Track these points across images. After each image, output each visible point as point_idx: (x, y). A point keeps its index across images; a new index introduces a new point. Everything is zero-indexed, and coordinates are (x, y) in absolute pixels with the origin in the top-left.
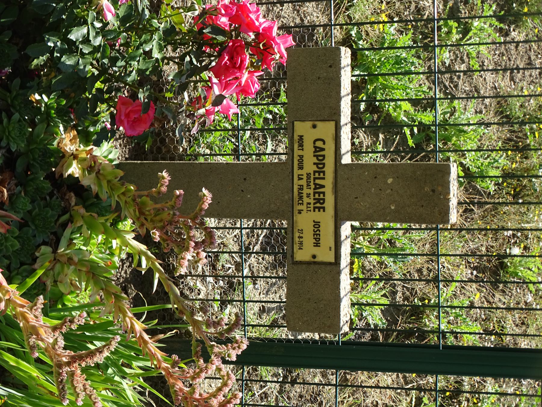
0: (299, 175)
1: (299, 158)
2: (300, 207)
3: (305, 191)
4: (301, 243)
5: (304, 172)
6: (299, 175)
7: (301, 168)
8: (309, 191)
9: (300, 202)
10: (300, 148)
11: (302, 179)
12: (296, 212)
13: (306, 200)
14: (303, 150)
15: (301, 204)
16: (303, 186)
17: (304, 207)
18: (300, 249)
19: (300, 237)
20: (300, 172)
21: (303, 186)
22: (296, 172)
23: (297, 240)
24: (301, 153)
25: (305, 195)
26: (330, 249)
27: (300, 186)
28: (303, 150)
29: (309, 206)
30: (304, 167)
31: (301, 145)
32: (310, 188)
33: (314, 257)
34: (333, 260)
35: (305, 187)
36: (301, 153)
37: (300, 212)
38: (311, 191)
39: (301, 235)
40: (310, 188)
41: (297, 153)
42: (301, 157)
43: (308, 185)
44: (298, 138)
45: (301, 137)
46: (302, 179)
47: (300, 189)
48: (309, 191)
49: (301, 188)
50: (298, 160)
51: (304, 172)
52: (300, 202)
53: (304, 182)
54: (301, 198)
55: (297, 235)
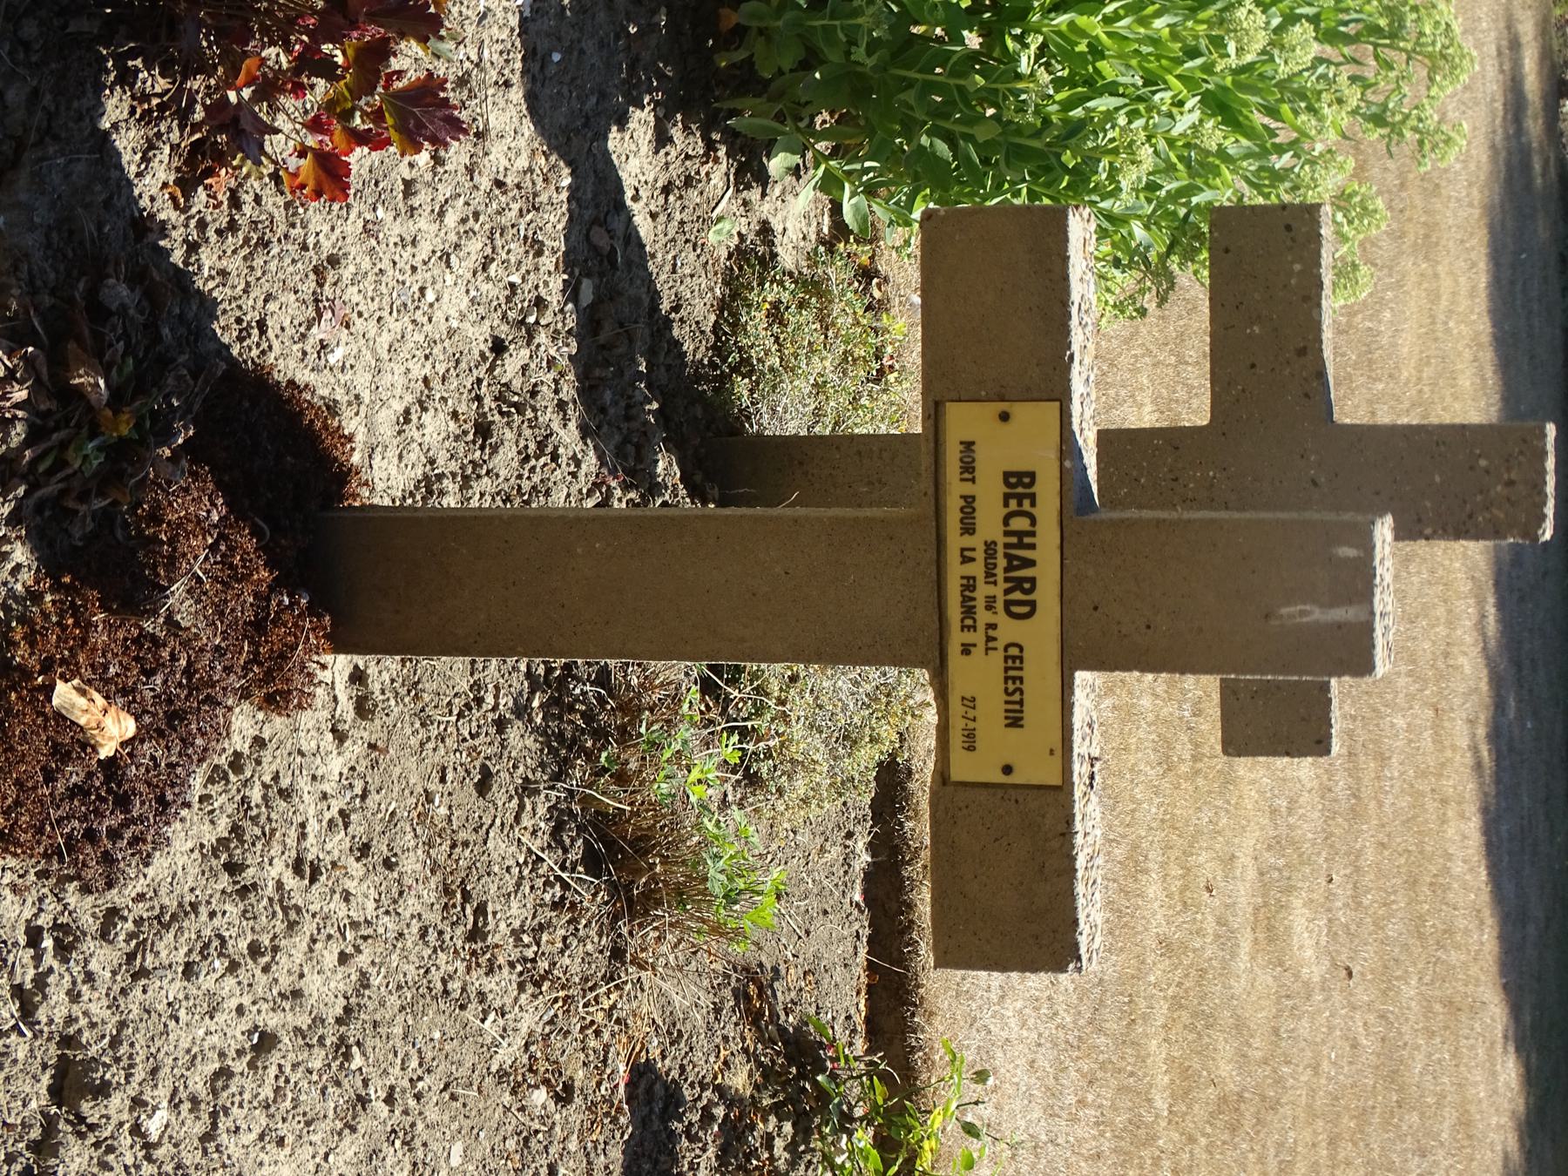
0: (963, 550)
1: (962, 503)
2: (969, 637)
3: (982, 591)
4: (970, 736)
5: (976, 541)
6: (963, 550)
7: (968, 529)
8: (991, 590)
9: (969, 622)
10: (966, 476)
11: (973, 560)
12: (954, 649)
13: (983, 617)
14: (973, 480)
15: (969, 628)
16: (974, 578)
17: (978, 637)
20: (968, 541)
21: (974, 578)
22: (955, 540)
24: (967, 489)
25: (980, 604)
26: (1052, 752)
27: (968, 578)
28: (973, 480)
29: (991, 633)
30: (978, 527)
31: (968, 468)
32: (995, 583)
33: (1007, 770)
34: (1059, 783)
36: (967, 489)
37: (966, 650)
38: (998, 591)
39: (971, 714)
40: (995, 583)
41: (955, 489)
42: (969, 500)
43: (990, 574)
44: (961, 447)
45: (968, 445)
46: (973, 560)
48: (991, 590)
49: (969, 585)
50: (962, 510)
51: (976, 541)
52: (969, 622)
53: (976, 568)
54: (969, 611)
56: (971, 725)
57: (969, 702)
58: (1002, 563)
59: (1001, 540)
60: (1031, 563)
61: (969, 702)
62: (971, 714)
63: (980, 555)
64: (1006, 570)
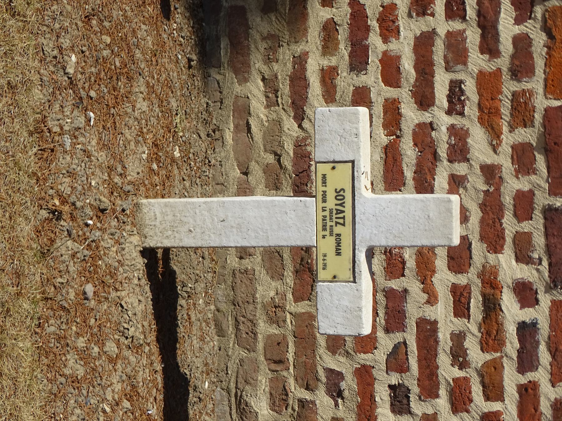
7: (324, 201)
14: (326, 186)
18: (324, 269)
19: (324, 260)
20: (324, 205)
23: (320, 263)
24: (324, 189)
26: (350, 269)
28: (326, 186)
31: (324, 182)
35: (328, 218)
36: (324, 189)
39: (325, 258)
41: (321, 188)
42: (325, 192)
45: (324, 176)
47: (323, 220)
53: (327, 213)
55: (320, 258)
57: (325, 255)
58: (335, 212)
59: (334, 207)
60: (344, 212)
62: (325, 258)
63: (328, 211)
64: (336, 214)
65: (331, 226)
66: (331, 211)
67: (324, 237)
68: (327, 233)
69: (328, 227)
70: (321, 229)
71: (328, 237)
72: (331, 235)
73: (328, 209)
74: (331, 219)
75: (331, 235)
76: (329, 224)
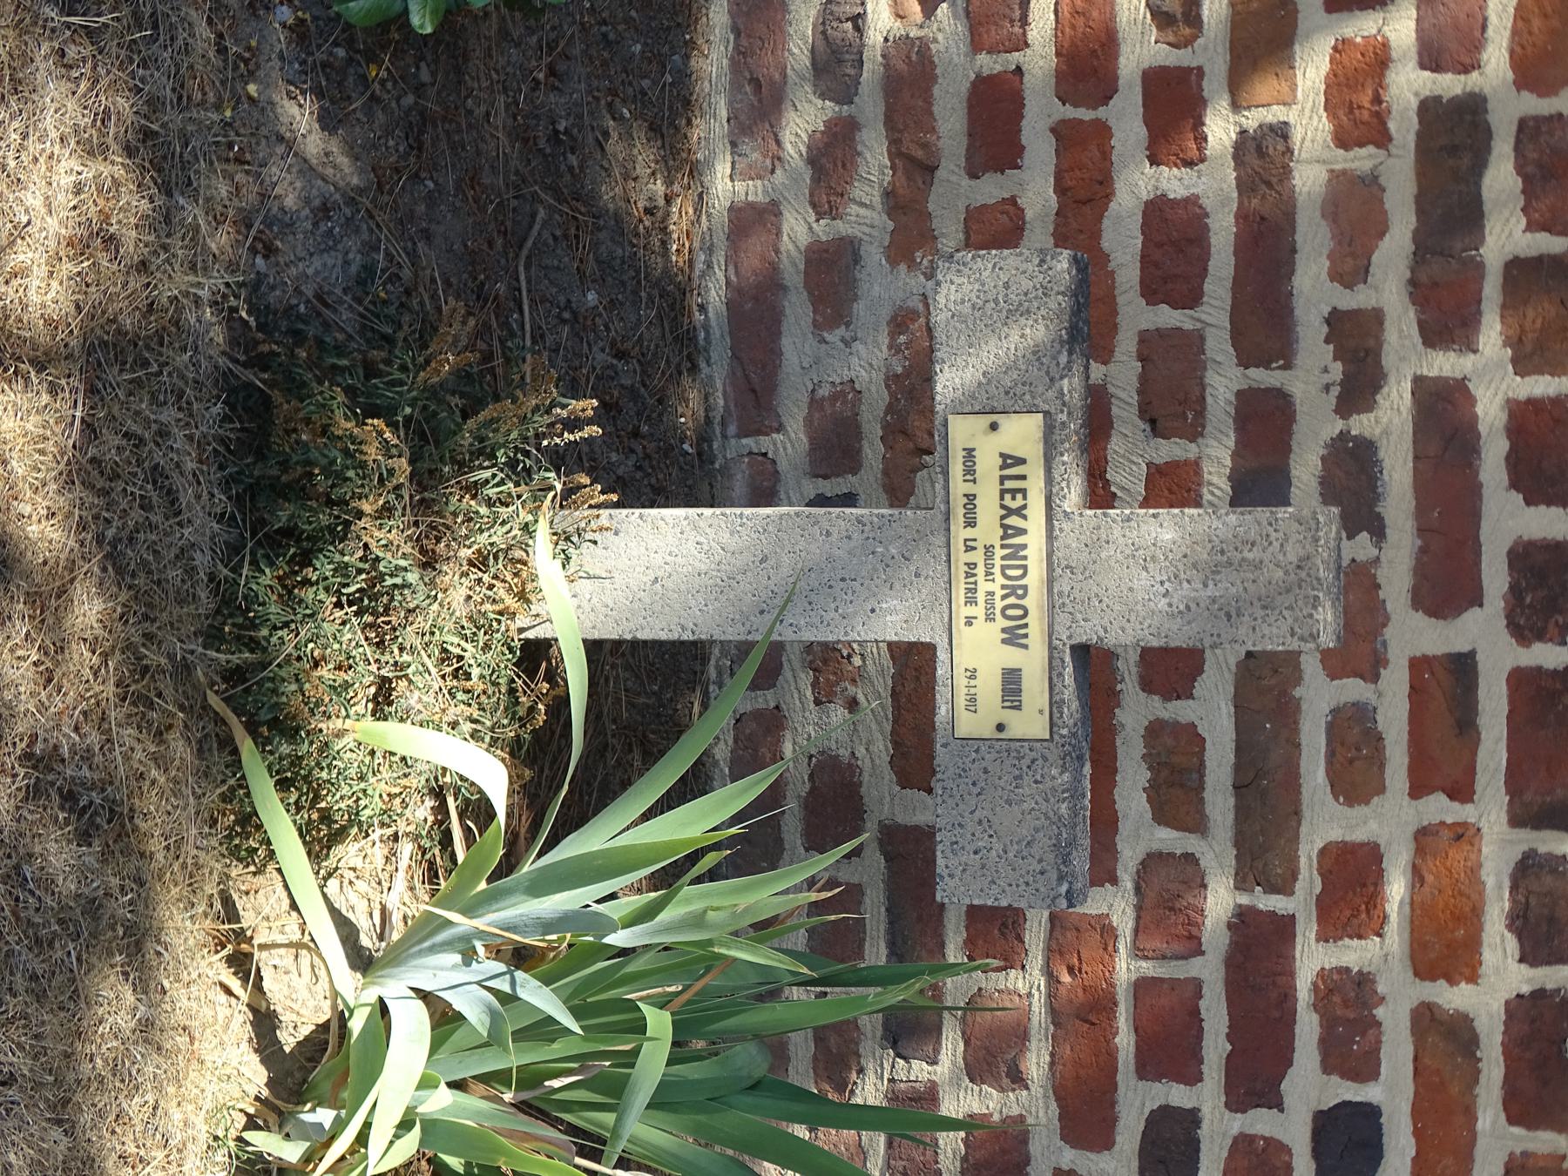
4: (972, 700)
7: (971, 523)
14: (974, 481)
22: (960, 533)
24: (969, 488)
26: (1041, 712)
28: (974, 481)
31: (970, 471)
36: (969, 488)
41: (959, 487)
42: (971, 498)
45: (970, 453)
53: (978, 557)
56: (973, 691)
57: (972, 674)
61: (972, 674)
62: (973, 683)
65: (991, 594)
66: (989, 550)
67: (969, 622)
68: (979, 611)
69: (981, 597)
70: (962, 600)
71: (980, 623)
72: (990, 618)
73: (979, 545)
74: (988, 574)
75: (990, 618)
76: (983, 586)
